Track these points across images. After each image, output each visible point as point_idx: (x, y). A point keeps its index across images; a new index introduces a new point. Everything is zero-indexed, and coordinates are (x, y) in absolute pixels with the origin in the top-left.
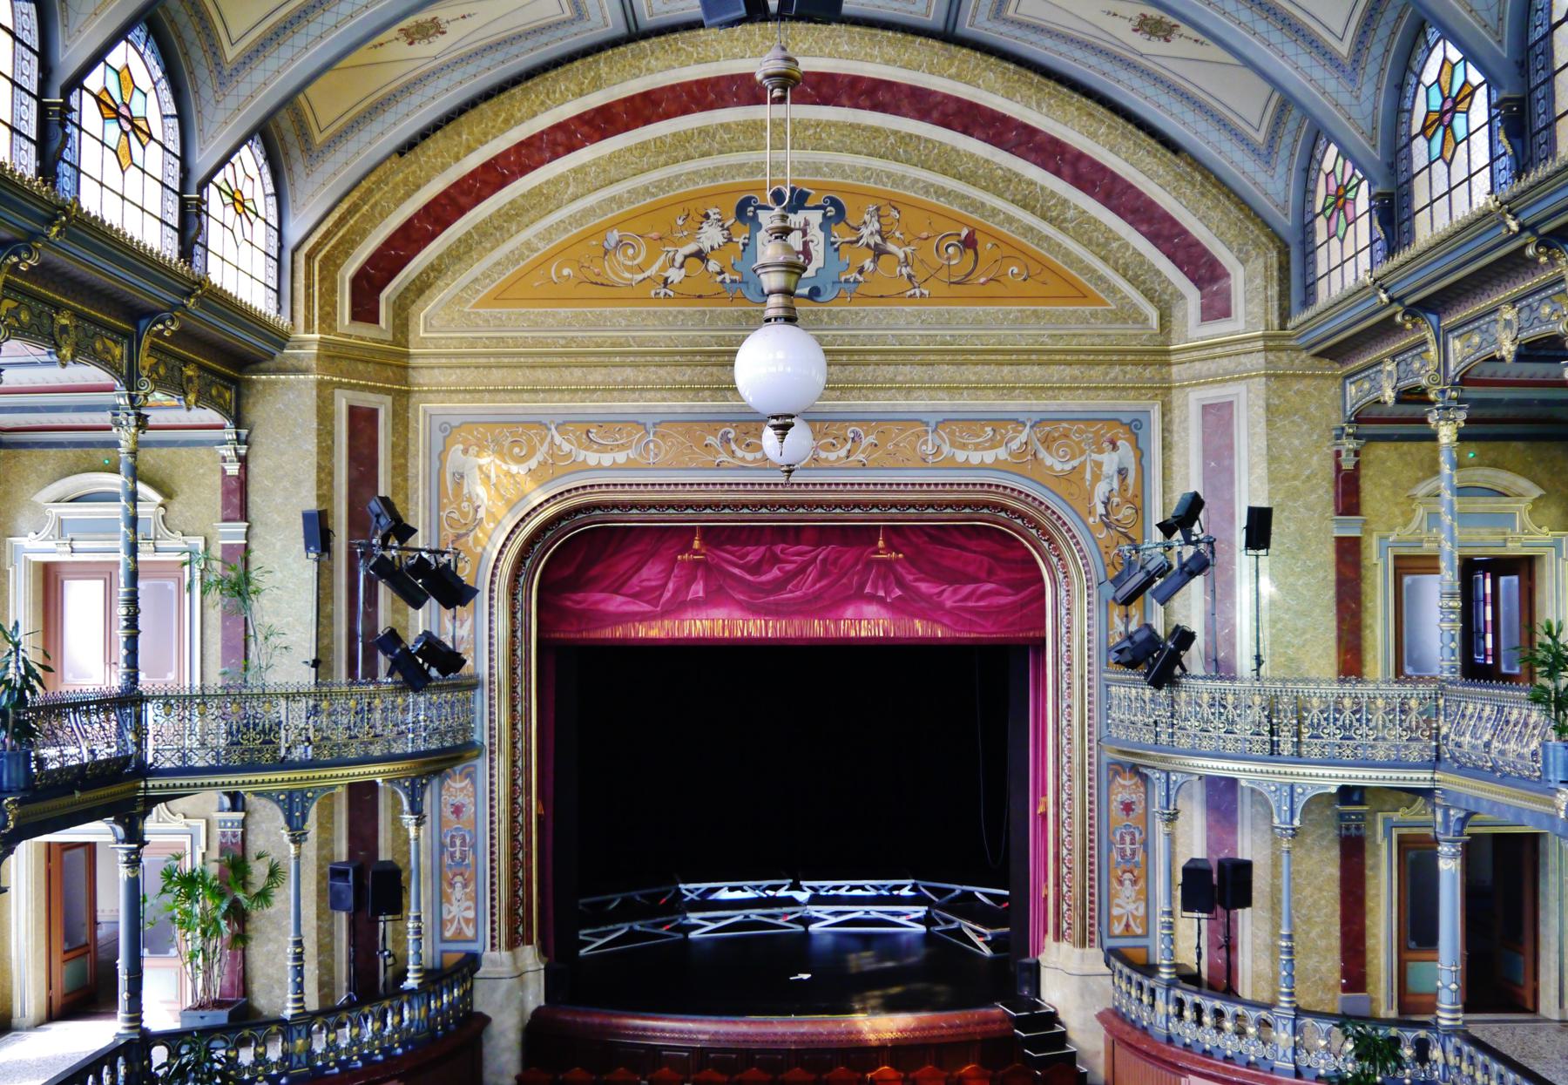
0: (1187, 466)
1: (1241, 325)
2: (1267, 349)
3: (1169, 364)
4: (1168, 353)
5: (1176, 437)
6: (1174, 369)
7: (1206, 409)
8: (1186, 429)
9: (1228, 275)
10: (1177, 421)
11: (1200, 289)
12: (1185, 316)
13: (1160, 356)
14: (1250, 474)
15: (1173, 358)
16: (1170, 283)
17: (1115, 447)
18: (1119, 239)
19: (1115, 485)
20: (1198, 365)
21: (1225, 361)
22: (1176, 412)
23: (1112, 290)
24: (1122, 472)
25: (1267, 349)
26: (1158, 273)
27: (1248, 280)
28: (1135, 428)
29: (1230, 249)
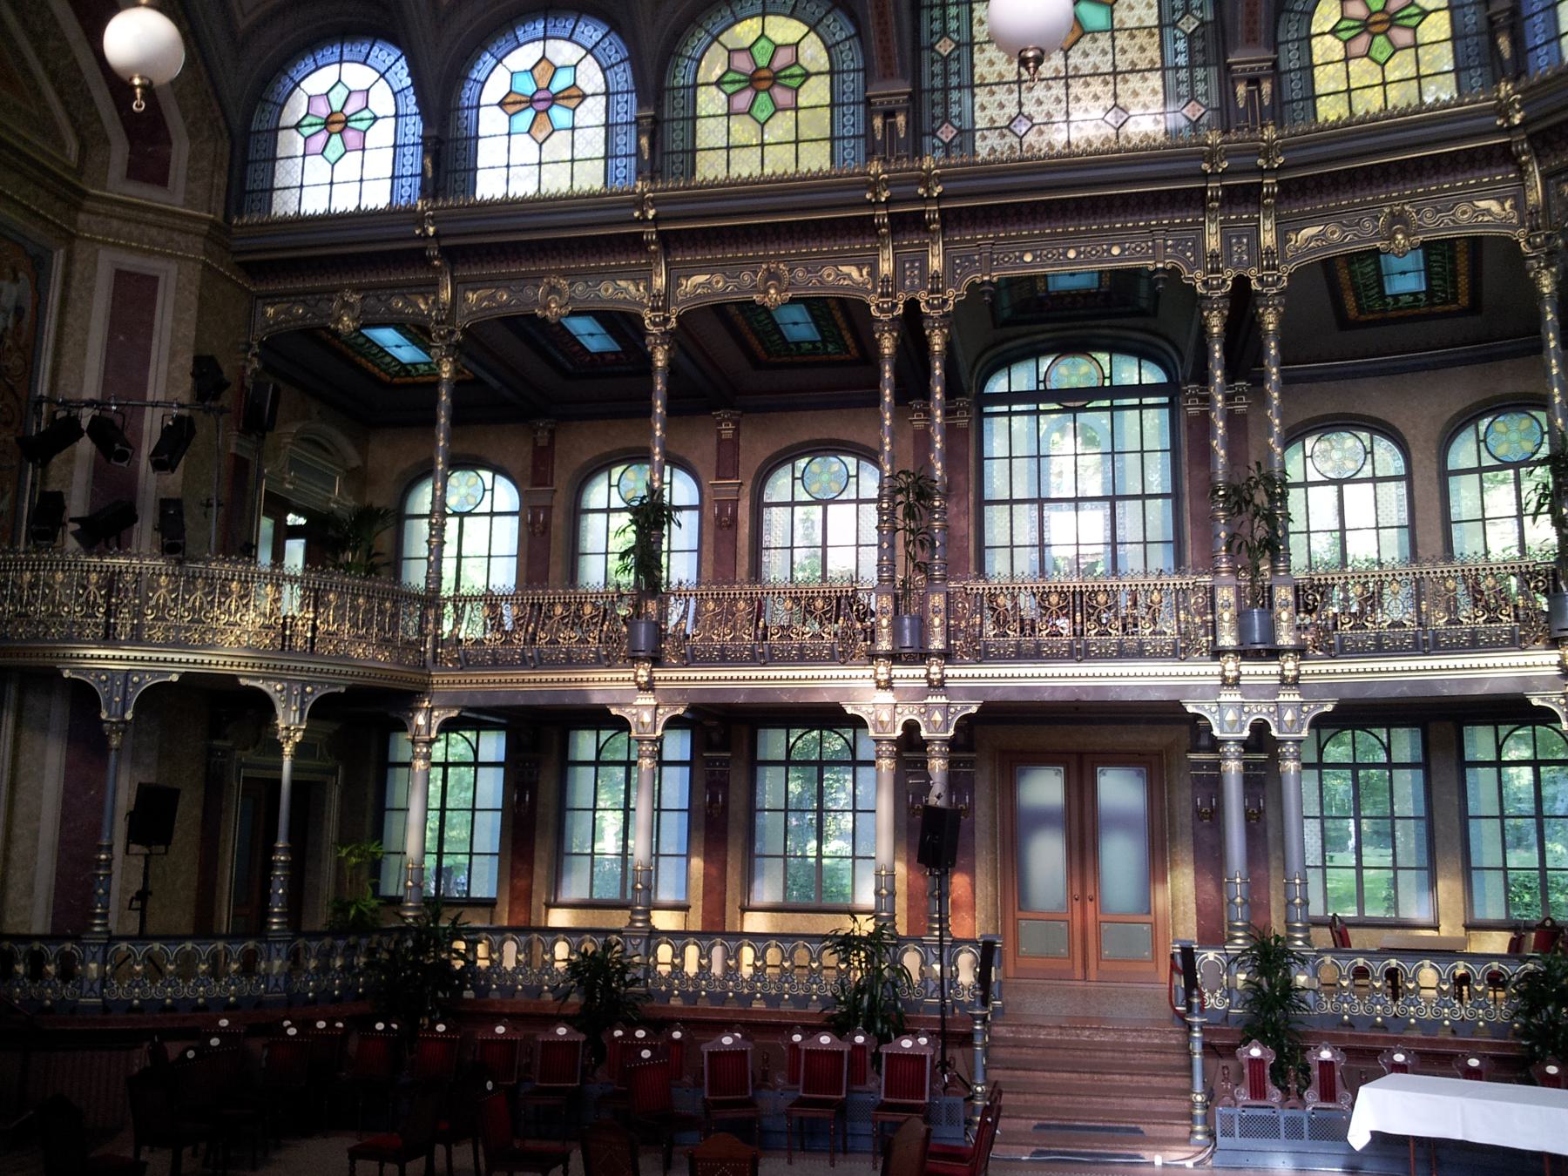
0: (86, 330)
1: (180, 198)
2: (208, 236)
3: (78, 208)
4: (85, 195)
5: (73, 294)
6: (82, 217)
7: (121, 276)
8: (91, 290)
9: (170, 143)
10: (77, 276)
11: (131, 143)
12: (106, 164)
13: (73, 197)
14: (171, 361)
15: (88, 204)
16: (99, 120)
17: (16, 280)
18: (63, 39)
19: (10, 324)
20: (115, 223)
21: (154, 232)
22: (78, 267)
23: (39, 94)
24: (19, 311)
25: (208, 236)
26: (91, 101)
27: (194, 157)
28: (39, 267)
29: (185, 117)
